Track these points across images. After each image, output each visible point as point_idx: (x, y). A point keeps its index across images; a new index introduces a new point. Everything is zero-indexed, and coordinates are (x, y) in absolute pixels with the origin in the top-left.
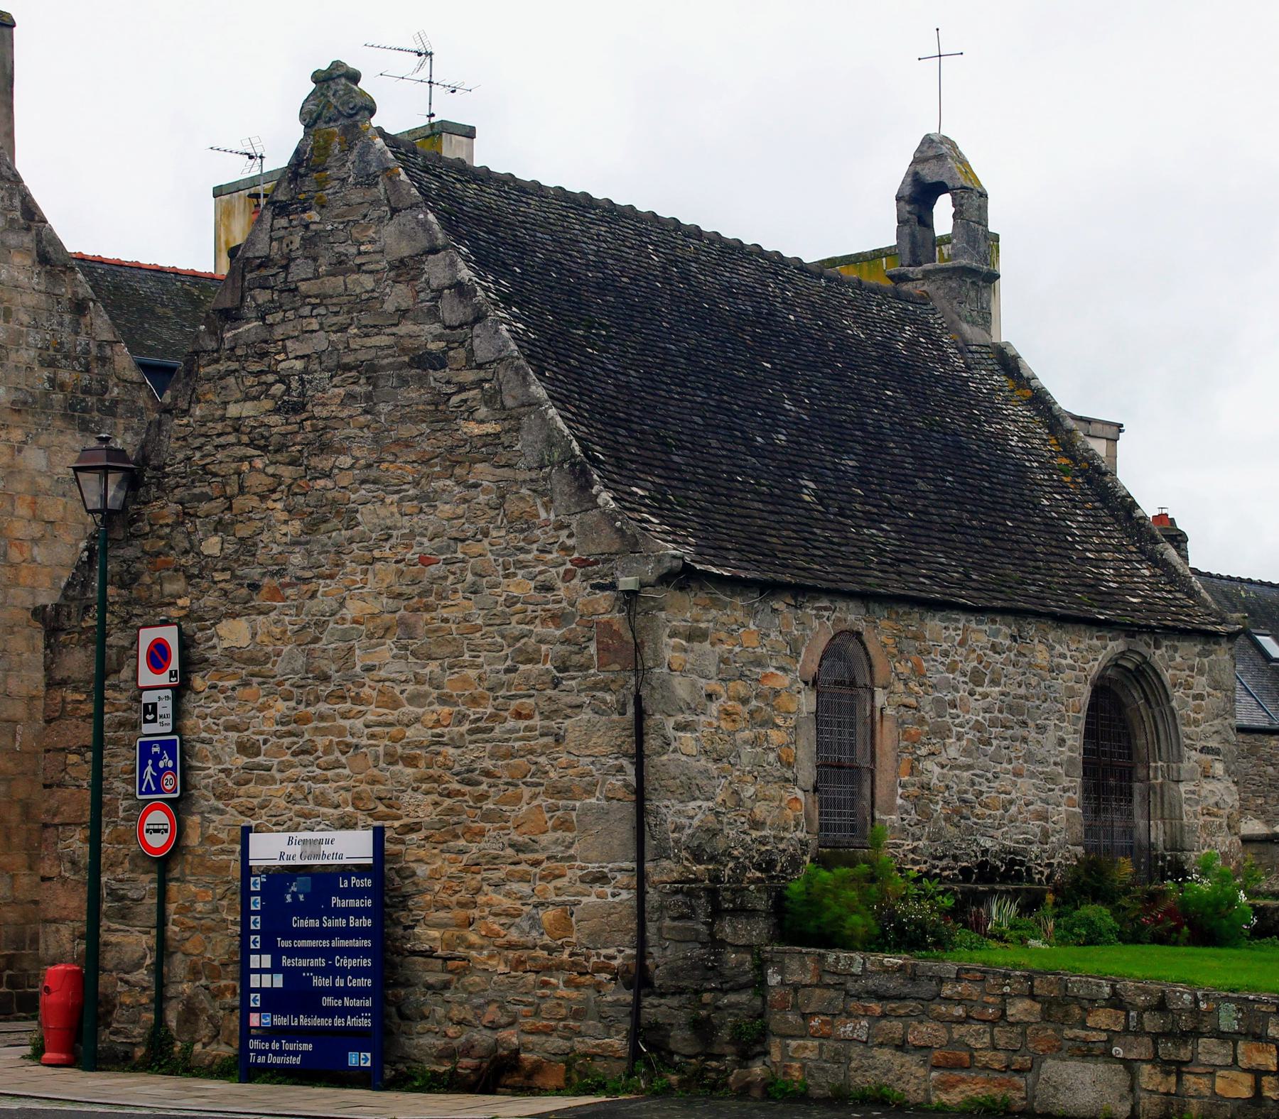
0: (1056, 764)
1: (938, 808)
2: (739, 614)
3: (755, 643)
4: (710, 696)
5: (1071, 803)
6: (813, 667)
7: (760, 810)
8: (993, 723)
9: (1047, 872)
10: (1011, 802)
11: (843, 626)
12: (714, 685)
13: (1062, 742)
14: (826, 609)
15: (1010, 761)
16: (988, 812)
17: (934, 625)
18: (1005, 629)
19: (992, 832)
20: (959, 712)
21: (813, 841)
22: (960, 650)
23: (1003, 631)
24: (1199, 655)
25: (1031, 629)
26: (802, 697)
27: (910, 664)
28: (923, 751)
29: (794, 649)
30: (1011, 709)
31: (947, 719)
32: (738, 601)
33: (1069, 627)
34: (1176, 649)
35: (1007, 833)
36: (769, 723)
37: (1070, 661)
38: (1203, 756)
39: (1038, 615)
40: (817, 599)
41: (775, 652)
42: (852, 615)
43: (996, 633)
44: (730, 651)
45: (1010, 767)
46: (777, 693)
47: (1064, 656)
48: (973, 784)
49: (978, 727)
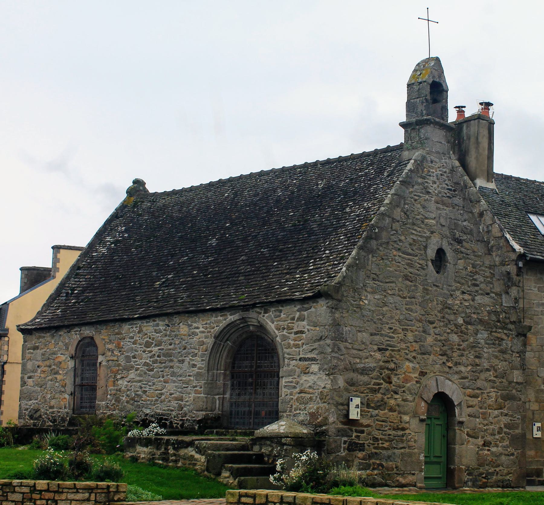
0: (189, 376)
1: (124, 398)
2: (49, 339)
3: (53, 347)
4: (38, 367)
5: (196, 392)
6: (73, 352)
7: (53, 402)
8: (155, 362)
9: (180, 423)
10: (162, 394)
11: (84, 336)
12: (40, 363)
13: (194, 366)
14: (77, 331)
15: (163, 377)
16: (148, 398)
17: (126, 327)
18: (161, 323)
19: (150, 407)
20: (137, 360)
21: (70, 412)
22: (138, 335)
23: (161, 324)
24: (298, 311)
25: (176, 319)
26: (69, 363)
27: (114, 345)
28: (119, 377)
29: (67, 346)
30: (164, 355)
31: (132, 363)
32: (48, 334)
33: (200, 315)
34: (281, 311)
35: (158, 406)
36: (57, 373)
37: (202, 329)
38: (301, 363)
39: (178, 313)
40: (74, 328)
41: (60, 349)
42: (87, 332)
43: (158, 325)
44: (45, 351)
45: (162, 379)
46: (60, 363)
47: (198, 328)
48: (141, 388)
49: (146, 364)
